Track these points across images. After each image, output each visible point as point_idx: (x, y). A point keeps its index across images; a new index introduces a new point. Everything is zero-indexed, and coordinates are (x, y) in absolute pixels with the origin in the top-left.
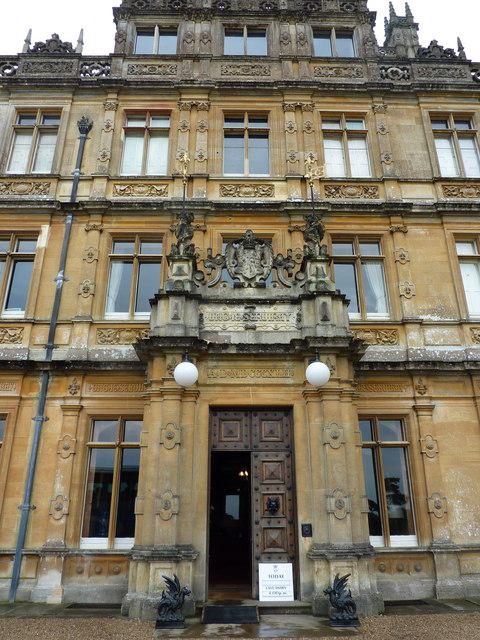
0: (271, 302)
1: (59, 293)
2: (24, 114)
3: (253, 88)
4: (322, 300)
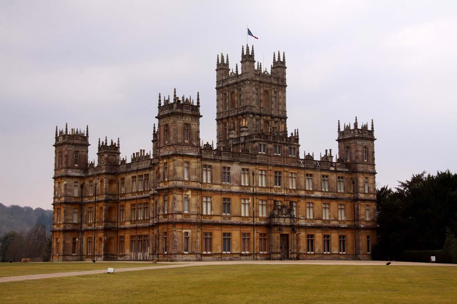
0: (287, 218)
2: (243, 169)
3: (280, 166)
4: (294, 219)
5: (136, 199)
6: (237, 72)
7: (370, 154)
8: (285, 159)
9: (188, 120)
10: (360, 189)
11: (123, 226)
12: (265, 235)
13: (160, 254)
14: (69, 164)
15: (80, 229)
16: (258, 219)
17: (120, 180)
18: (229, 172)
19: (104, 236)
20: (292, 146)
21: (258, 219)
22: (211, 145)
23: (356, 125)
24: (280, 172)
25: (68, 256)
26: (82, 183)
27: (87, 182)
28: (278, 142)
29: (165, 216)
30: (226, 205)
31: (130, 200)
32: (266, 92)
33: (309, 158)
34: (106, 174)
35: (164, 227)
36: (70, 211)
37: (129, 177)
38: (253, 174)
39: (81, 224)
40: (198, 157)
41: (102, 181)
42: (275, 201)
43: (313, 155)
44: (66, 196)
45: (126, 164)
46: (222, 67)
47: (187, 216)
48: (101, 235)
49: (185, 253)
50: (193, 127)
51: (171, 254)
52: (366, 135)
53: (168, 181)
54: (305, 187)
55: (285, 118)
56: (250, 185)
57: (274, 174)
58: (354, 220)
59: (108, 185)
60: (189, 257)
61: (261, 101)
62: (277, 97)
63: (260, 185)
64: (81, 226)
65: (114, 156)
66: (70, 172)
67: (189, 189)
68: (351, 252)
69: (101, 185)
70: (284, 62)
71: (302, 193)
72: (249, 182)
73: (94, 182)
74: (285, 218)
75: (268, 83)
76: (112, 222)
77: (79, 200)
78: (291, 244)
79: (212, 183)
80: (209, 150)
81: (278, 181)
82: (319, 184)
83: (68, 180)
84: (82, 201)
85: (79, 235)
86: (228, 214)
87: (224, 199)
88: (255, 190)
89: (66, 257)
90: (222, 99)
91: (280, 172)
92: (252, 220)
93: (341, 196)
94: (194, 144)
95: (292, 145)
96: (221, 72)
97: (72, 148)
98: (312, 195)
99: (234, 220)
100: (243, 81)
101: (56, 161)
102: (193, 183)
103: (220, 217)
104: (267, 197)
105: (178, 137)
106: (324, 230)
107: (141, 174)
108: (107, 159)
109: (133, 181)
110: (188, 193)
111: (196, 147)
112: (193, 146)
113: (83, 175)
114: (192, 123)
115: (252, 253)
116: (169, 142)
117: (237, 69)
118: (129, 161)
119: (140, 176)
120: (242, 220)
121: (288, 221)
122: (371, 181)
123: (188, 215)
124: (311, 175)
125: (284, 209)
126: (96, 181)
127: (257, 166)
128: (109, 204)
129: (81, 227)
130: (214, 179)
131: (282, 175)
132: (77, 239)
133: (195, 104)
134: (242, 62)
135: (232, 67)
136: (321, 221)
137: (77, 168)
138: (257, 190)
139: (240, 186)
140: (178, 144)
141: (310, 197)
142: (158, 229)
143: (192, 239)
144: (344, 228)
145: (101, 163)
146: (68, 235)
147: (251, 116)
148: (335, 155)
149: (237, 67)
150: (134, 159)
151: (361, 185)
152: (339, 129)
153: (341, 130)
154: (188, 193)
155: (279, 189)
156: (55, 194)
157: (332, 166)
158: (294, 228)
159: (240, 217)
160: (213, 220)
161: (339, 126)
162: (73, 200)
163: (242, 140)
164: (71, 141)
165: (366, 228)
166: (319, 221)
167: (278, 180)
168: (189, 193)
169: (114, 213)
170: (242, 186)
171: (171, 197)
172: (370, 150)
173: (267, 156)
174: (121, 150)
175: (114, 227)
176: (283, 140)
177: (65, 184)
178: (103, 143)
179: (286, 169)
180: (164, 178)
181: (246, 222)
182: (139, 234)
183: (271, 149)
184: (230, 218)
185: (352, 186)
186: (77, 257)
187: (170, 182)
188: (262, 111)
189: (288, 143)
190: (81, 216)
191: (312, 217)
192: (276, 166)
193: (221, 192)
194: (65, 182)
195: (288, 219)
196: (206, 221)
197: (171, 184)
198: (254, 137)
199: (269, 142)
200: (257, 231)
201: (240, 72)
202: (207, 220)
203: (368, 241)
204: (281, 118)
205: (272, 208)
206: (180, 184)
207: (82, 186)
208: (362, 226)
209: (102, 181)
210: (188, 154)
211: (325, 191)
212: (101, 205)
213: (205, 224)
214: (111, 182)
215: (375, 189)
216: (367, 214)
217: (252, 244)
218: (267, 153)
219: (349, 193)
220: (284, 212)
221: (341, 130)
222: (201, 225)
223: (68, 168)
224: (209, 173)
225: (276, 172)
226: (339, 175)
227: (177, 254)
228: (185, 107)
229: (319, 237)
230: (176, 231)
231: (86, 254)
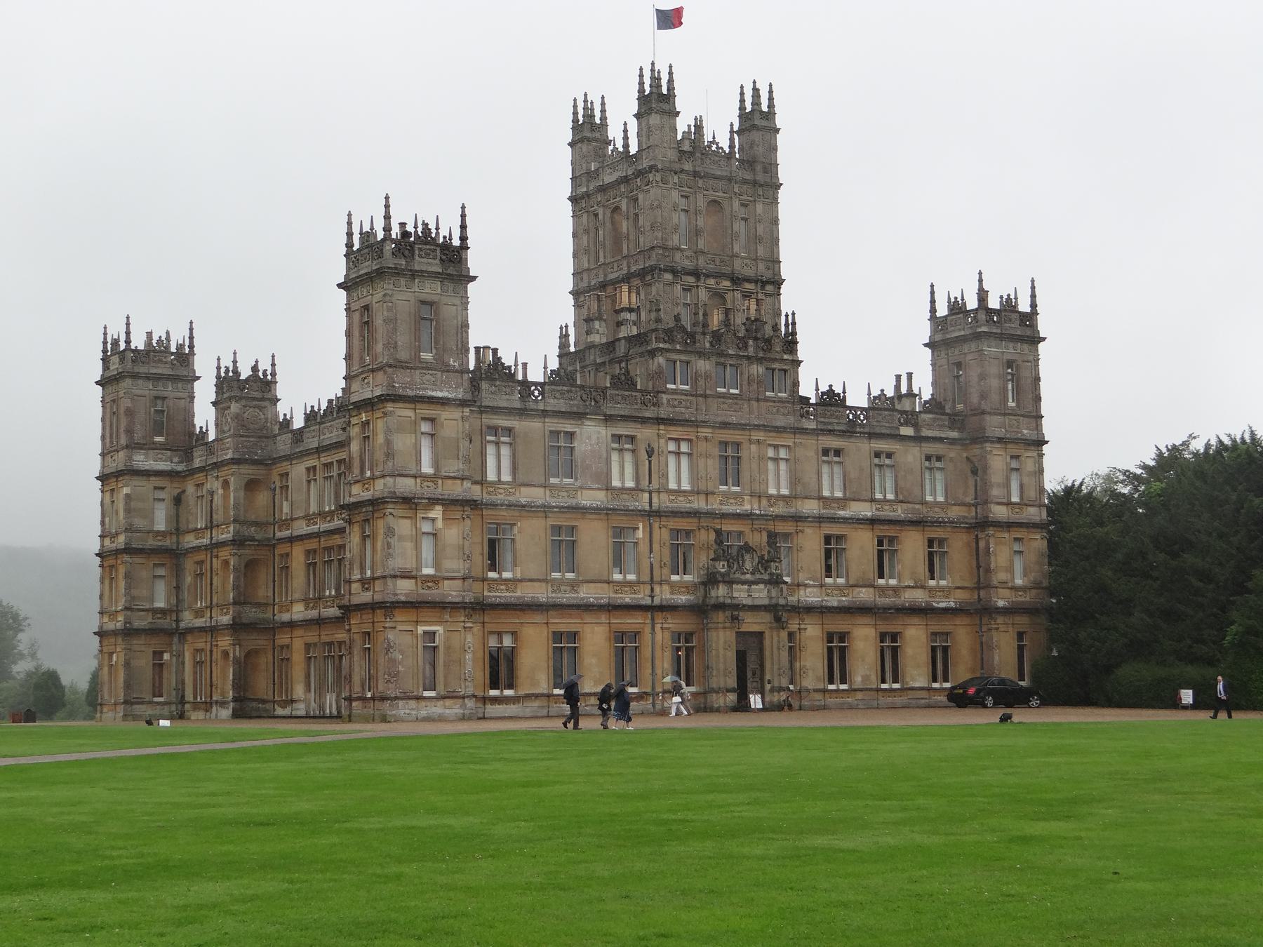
0: (756, 583)
1: (652, 565)
5: (317, 535)
8: (755, 404)
9: (431, 289)
10: (995, 492)
11: (286, 617)
12: (689, 636)
14: (138, 436)
16: (666, 588)
17: (277, 479)
18: (572, 448)
20: (776, 365)
21: (666, 588)
22: (510, 367)
23: (982, 295)
24: (738, 445)
25: (142, 703)
26: (177, 491)
27: (191, 489)
28: (731, 352)
29: (366, 583)
30: (564, 546)
31: (301, 538)
33: (832, 400)
34: (234, 461)
36: (144, 574)
37: (298, 471)
39: (174, 611)
40: (463, 403)
41: (226, 484)
42: (718, 533)
43: (844, 392)
44: (129, 529)
45: (293, 431)
46: (588, 131)
48: (225, 642)
49: (427, 694)
50: (448, 311)
51: (383, 699)
52: (1014, 327)
53: (373, 478)
54: (820, 489)
55: (778, 283)
56: (641, 487)
57: (716, 451)
58: (979, 587)
59: (242, 493)
60: (437, 709)
61: (698, 232)
63: (672, 485)
65: (261, 408)
66: (142, 460)
69: (221, 495)
71: (810, 507)
72: (637, 479)
73: (208, 486)
74: (750, 583)
76: (259, 605)
77: (168, 543)
79: (516, 483)
81: (730, 471)
83: (138, 482)
84: (178, 543)
86: (570, 576)
87: (557, 529)
88: (655, 500)
89: (135, 706)
90: (587, 231)
91: (738, 445)
92: (648, 592)
93: (938, 514)
95: (776, 360)
96: (585, 147)
98: (842, 513)
99: (588, 593)
101: (104, 428)
102: (450, 482)
103: (544, 585)
104: (696, 520)
105: (400, 343)
108: (237, 417)
109: (309, 482)
110: (432, 514)
111: (457, 371)
112: (447, 369)
113: (180, 468)
114: (445, 300)
115: (649, 690)
116: (374, 358)
117: (626, 138)
118: (298, 423)
119: (328, 466)
121: (761, 594)
122: (1030, 466)
123: (434, 580)
124: (837, 453)
125: (747, 557)
126: (213, 484)
127: (662, 427)
128: (247, 552)
129: (177, 621)
131: (744, 454)
132: (166, 656)
134: (638, 116)
135: (614, 133)
136: (872, 590)
139: (609, 488)
140: (399, 365)
141: (833, 520)
144: (946, 611)
145: (223, 432)
146: (138, 643)
147: (668, 277)
148: (924, 387)
149: (625, 131)
150: (311, 417)
151: (996, 477)
152: (933, 310)
153: (938, 315)
154: (432, 514)
155: (736, 496)
156: (103, 523)
157: (906, 424)
158: (778, 613)
160: (519, 594)
161: (933, 302)
162: (151, 543)
163: (621, 349)
164: (143, 369)
167: (731, 465)
168: (437, 512)
169: (263, 576)
170: (614, 489)
171: (380, 524)
172: (1026, 373)
173: (696, 396)
174: (280, 391)
176: (746, 347)
177: (127, 495)
179: (756, 435)
181: (627, 599)
182: (325, 639)
183: (707, 376)
184: (573, 585)
185: (971, 482)
188: (701, 261)
189: (761, 355)
190: (178, 588)
192: (725, 425)
193: (545, 510)
194: (126, 490)
195: (762, 586)
197: (380, 487)
199: (701, 354)
201: (633, 149)
203: (1021, 649)
204: (764, 283)
205: (712, 555)
206: (406, 485)
207: (178, 501)
208: (1001, 603)
209: (226, 484)
211: (885, 501)
212: (225, 553)
213: (495, 607)
214: (251, 486)
215: (1042, 490)
216: (1017, 568)
217: (649, 665)
219: (964, 504)
220: (748, 565)
221: (938, 315)
222: (480, 607)
223: (132, 446)
224: (505, 451)
226: (930, 448)
227: (402, 699)
228: (420, 249)
231: (191, 699)
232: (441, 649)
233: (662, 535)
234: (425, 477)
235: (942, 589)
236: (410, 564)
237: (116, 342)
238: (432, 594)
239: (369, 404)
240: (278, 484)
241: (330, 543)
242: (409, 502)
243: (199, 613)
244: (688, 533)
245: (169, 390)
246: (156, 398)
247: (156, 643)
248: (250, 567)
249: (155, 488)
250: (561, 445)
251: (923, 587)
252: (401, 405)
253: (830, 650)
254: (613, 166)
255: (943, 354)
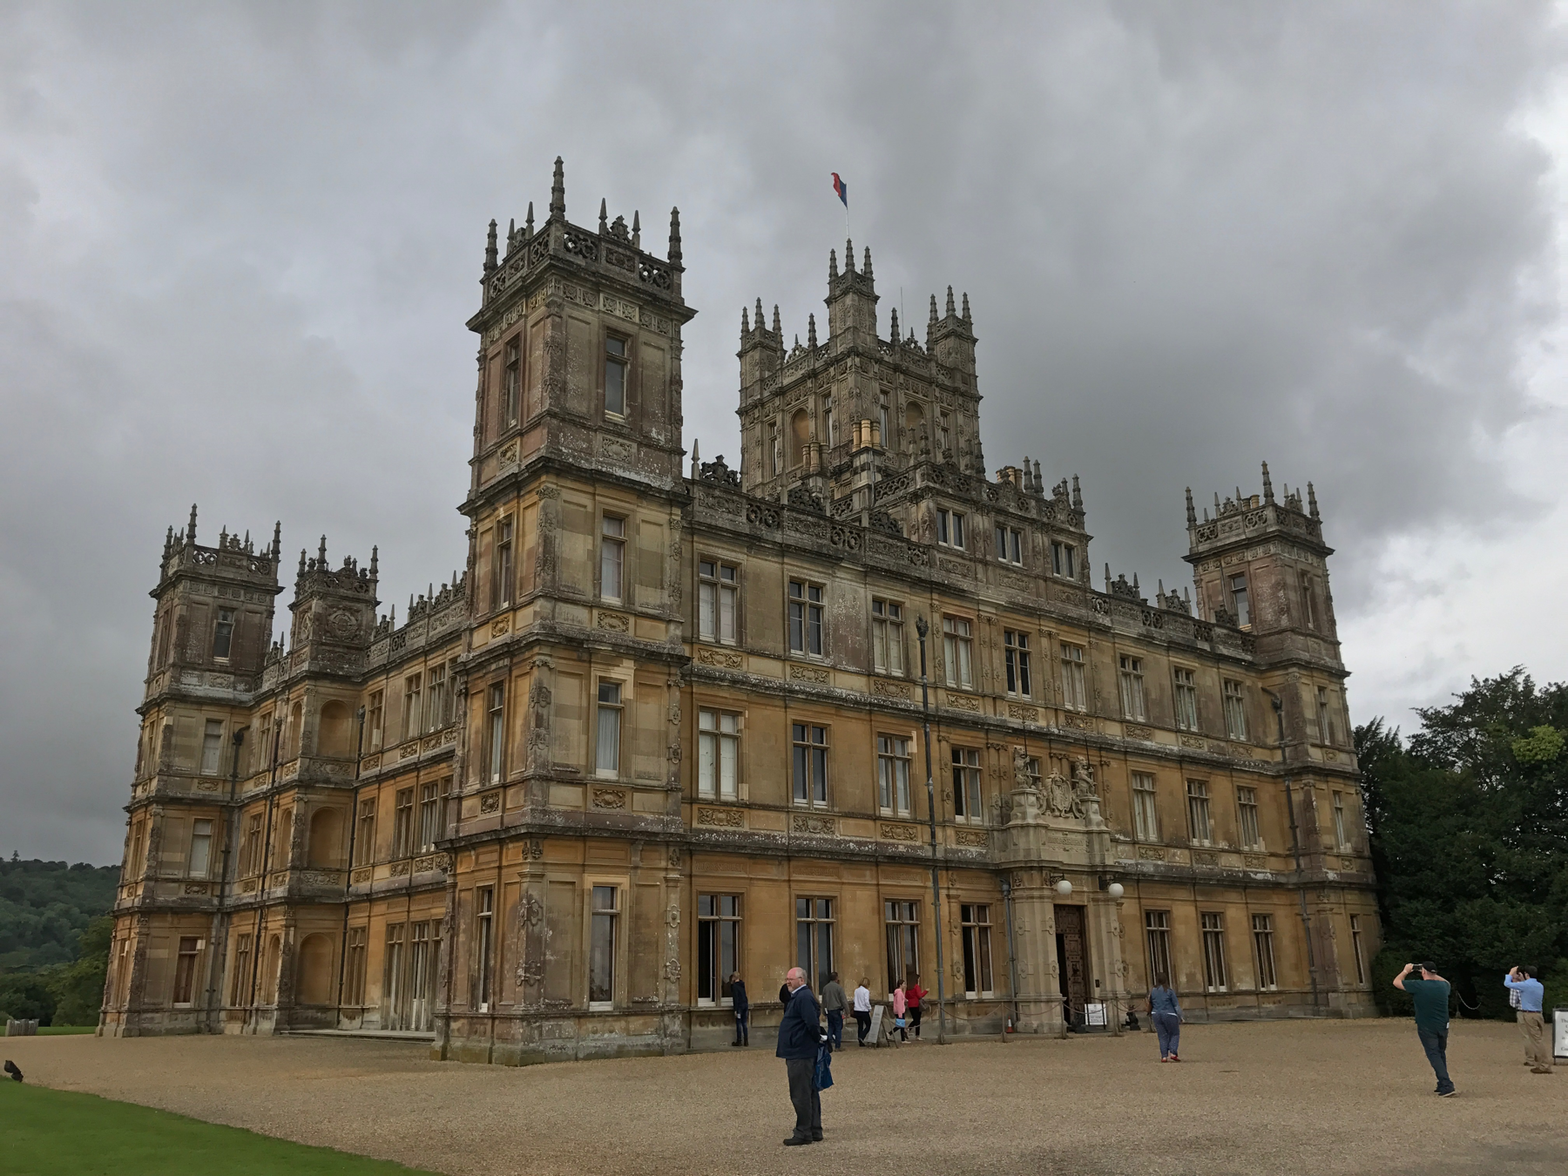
2: (878, 602)
5: (416, 767)
6: (813, 339)
7: (1320, 600)
9: (624, 313)
11: (363, 887)
13: (457, 1018)
14: (190, 653)
15: (216, 901)
17: (367, 701)
19: (287, 927)
21: (950, 832)
22: (734, 473)
24: (1023, 637)
25: (157, 1011)
26: (237, 727)
27: (256, 723)
29: (489, 797)
32: (915, 406)
33: (1123, 594)
34: (312, 676)
35: (482, 858)
36: (182, 833)
37: (396, 684)
38: (919, 628)
39: (220, 883)
44: (166, 771)
47: (608, 797)
48: (276, 922)
50: (649, 355)
52: (1301, 531)
53: (514, 609)
54: (1121, 710)
56: (913, 677)
58: (1294, 853)
59: (317, 719)
62: (952, 432)
63: (951, 683)
64: (223, 891)
65: (354, 612)
66: (194, 684)
67: (622, 651)
68: (1294, 984)
70: (966, 322)
71: (1113, 731)
72: (907, 663)
75: (921, 378)
77: (219, 793)
78: (1101, 958)
80: (726, 491)
82: (1167, 701)
83: (181, 710)
84: (233, 792)
85: (209, 929)
86: (820, 804)
87: (801, 727)
88: (931, 699)
90: (761, 443)
91: (1023, 637)
92: (927, 838)
94: (654, 434)
95: (1061, 531)
96: (756, 355)
97: (207, 596)
98: (1148, 743)
99: (848, 833)
100: (836, 361)
101: (153, 650)
102: (647, 623)
105: (571, 386)
106: (1203, 893)
107: (439, 661)
108: (318, 618)
109: (409, 697)
110: (616, 673)
111: (662, 449)
112: (647, 443)
113: (246, 697)
114: (644, 336)
117: (812, 330)
120: (885, 835)
122: (1334, 703)
123: (617, 791)
124: (1136, 662)
126: (283, 710)
128: (319, 798)
129: (222, 897)
130: (750, 629)
132: (200, 945)
133: (662, 254)
134: (829, 302)
135: (793, 336)
137: (223, 670)
138: (939, 701)
139: (870, 674)
142: (455, 875)
143: (635, 929)
146: (158, 926)
149: (812, 323)
155: (1025, 707)
156: (138, 769)
159: (876, 818)
162: (195, 791)
165: (1341, 886)
166: (1179, 852)
167: (1018, 668)
168: (624, 672)
169: (338, 831)
170: (878, 675)
172: (1319, 590)
173: (975, 560)
175: (334, 892)
177: (167, 726)
178: (312, 565)
179: (1048, 626)
180: (495, 600)
182: (417, 916)
184: (827, 820)
186: (192, 1017)
187: (520, 614)
191: (1153, 837)
196: (711, 832)
198: (914, 479)
199: (980, 507)
200: (952, 892)
201: (823, 338)
202: (719, 828)
206: (576, 618)
207: (239, 739)
208: (1331, 876)
209: (298, 707)
210: (619, 473)
214: (331, 710)
216: (1341, 826)
218: (972, 546)
219: (1264, 747)
222: (687, 848)
223: (183, 666)
225: (1009, 633)
228: (610, 252)
229: (1184, 915)
230: (542, 876)
232: (625, 918)
233: (941, 751)
234: (607, 609)
235: (1257, 856)
236: (575, 757)
237: (179, 540)
238: (615, 814)
239: (514, 486)
240: (368, 708)
241: (432, 777)
242: (577, 647)
243: (248, 886)
244: (972, 752)
245: (241, 599)
246: (221, 607)
247: (187, 926)
248: (319, 820)
249: (209, 721)
250: (803, 603)
251: (1238, 852)
252: (569, 484)
253: (1205, 934)
254: (794, 365)
255: (1212, 568)
